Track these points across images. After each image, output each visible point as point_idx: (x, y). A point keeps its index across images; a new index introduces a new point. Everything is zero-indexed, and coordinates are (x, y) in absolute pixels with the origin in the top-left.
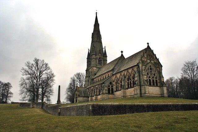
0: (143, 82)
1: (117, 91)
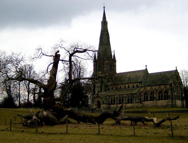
1: (145, 100)
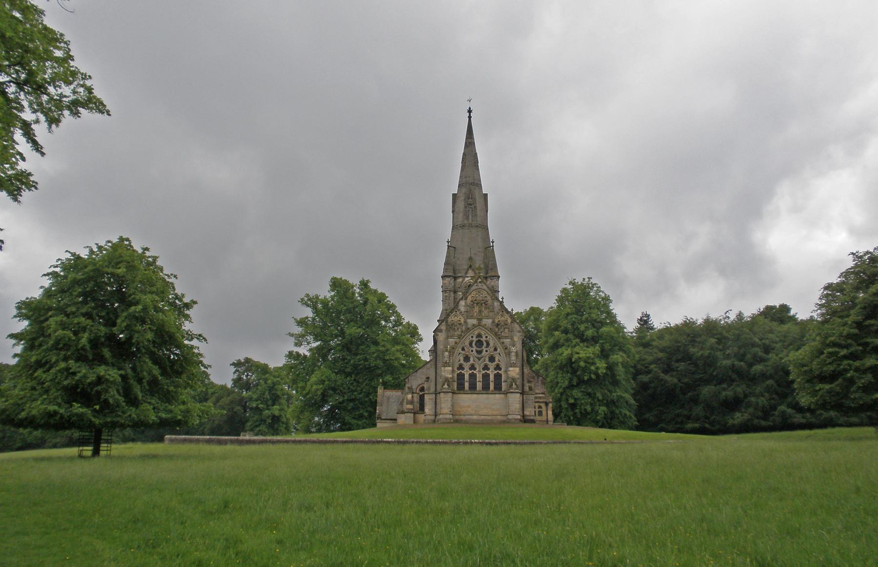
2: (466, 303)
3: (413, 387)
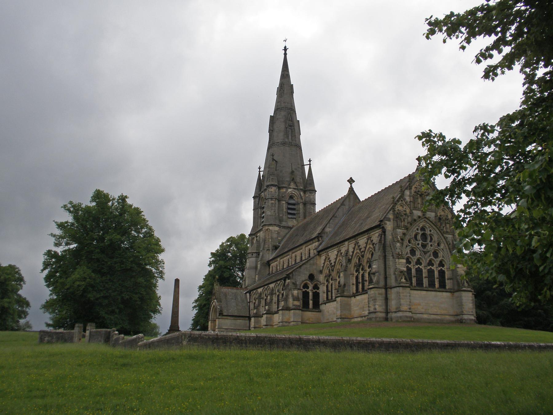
0: (393, 277)
2: (411, 193)
3: (298, 283)
